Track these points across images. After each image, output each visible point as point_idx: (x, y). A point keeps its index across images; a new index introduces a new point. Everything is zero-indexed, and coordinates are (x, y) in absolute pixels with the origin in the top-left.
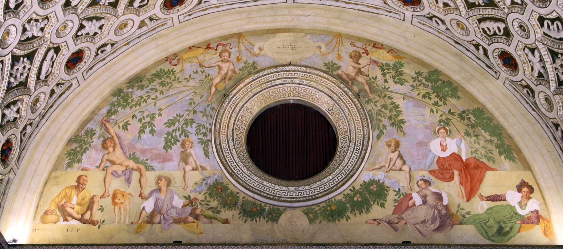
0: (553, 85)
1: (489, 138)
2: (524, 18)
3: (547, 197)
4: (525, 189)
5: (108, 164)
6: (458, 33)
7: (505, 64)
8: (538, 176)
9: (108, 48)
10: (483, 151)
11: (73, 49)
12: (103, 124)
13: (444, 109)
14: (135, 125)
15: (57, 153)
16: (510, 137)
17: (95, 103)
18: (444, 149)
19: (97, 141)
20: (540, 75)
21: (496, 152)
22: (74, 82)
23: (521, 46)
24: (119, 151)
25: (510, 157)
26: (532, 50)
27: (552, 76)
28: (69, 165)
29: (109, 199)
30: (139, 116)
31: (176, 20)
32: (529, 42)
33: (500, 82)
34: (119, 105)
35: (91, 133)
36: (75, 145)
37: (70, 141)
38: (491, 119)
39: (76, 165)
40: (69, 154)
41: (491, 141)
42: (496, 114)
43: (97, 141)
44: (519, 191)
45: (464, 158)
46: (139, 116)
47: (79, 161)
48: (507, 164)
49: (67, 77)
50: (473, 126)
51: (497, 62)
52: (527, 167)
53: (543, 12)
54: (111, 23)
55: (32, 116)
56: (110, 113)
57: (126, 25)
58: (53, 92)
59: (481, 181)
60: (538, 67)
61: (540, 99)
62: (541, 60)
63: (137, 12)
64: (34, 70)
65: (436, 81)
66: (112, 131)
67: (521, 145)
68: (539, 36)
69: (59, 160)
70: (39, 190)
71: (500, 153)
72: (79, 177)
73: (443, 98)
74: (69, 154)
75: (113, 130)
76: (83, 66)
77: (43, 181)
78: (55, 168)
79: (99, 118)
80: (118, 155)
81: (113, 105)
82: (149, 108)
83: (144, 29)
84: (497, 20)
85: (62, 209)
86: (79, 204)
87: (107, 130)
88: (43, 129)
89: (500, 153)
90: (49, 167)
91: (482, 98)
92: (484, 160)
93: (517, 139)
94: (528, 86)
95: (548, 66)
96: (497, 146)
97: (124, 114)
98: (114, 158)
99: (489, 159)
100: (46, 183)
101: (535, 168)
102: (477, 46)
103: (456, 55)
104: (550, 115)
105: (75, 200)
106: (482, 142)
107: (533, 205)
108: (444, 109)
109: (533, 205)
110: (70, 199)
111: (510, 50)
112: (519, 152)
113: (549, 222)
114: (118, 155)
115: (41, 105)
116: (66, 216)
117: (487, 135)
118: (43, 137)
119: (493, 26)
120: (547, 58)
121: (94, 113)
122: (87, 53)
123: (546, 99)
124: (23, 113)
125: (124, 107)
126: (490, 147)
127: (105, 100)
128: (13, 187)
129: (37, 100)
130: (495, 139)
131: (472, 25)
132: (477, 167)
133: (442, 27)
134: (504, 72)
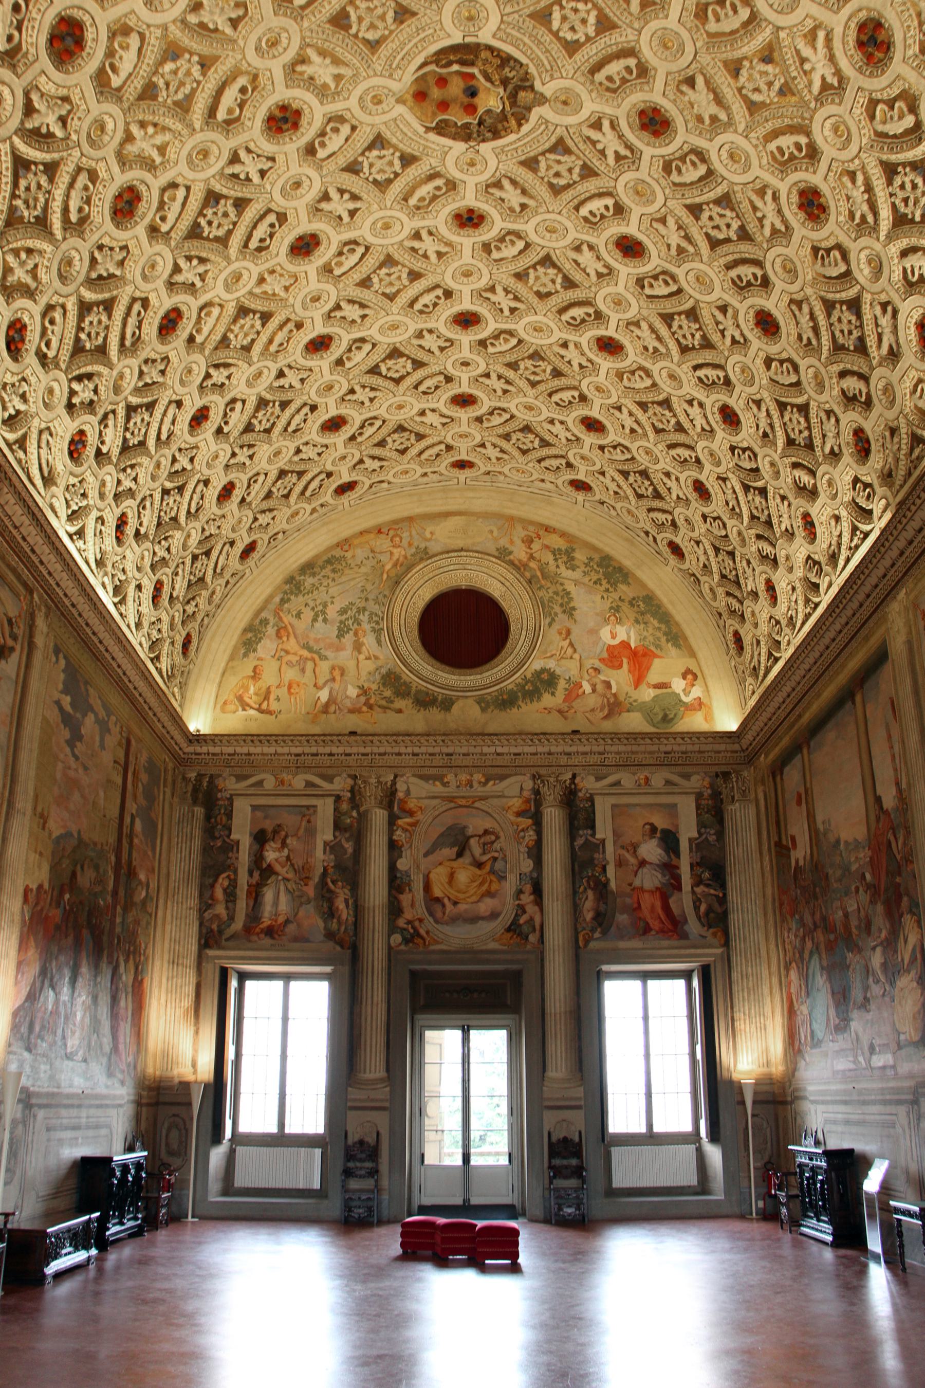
0: (716, 577)
1: (657, 625)
2: (689, 513)
3: (710, 684)
4: (690, 677)
5: (283, 653)
6: (629, 520)
7: (673, 553)
8: (702, 663)
9: (280, 536)
10: (651, 638)
11: (247, 540)
12: (276, 613)
13: (615, 596)
14: (308, 615)
15: (233, 643)
16: (677, 624)
17: (269, 591)
18: (614, 637)
19: (271, 630)
20: (705, 566)
21: (664, 639)
22: (248, 571)
23: (687, 538)
24: (292, 640)
25: (677, 645)
26: (698, 543)
27: (715, 569)
28: (245, 655)
29: (285, 689)
30: (312, 604)
31: (346, 504)
32: (695, 535)
33: (669, 569)
34: (292, 593)
35: (265, 622)
36: (250, 635)
37: (245, 631)
38: (659, 606)
39: (252, 655)
40: (245, 644)
41: (659, 629)
42: (665, 601)
43: (271, 630)
44: (684, 678)
45: (633, 646)
46: (312, 604)
47: (255, 650)
48: (673, 651)
49: (241, 568)
50: (643, 614)
51: (666, 551)
52: (693, 654)
53: (706, 510)
54: (283, 513)
55: (209, 608)
56: (283, 601)
57: (297, 513)
58: (228, 582)
59: (648, 668)
60: (702, 559)
61: (706, 589)
62: (705, 553)
63: (309, 501)
64: (212, 565)
65: (607, 567)
66: (285, 619)
67: (688, 633)
68: (703, 531)
69: (235, 650)
70: (218, 680)
71: (668, 641)
72: (255, 668)
73: (614, 584)
74: (245, 644)
75: (287, 619)
76: (255, 555)
77: (221, 671)
78: (232, 658)
79: (272, 607)
80: (292, 645)
81: (285, 593)
82: (321, 596)
83: (315, 515)
84: (664, 511)
85: (240, 699)
86: (256, 694)
87: (280, 619)
88: (218, 619)
89: (668, 641)
90: (226, 657)
91: (652, 584)
92: (652, 648)
93: (684, 626)
94: (694, 575)
95: (712, 559)
96: (665, 634)
97: (297, 602)
98: (288, 648)
99: (657, 646)
100: (224, 673)
101: (700, 655)
102: (647, 533)
103: (627, 540)
104: (714, 604)
105: (252, 690)
106: (650, 630)
107: (697, 692)
108: (615, 596)
109: (697, 692)
110: (247, 689)
111: (678, 540)
112: (686, 639)
113: (710, 708)
114: (292, 645)
115: (217, 598)
116: (245, 706)
117: (656, 623)
118: (219, 627)
119: (662, 517)
120: (711, 553)
121: (268, 601)
122: (260, 543)
123: (711, 589)
124: (201, 607)
125: (296, 595)
126: (659, 634)
127: (278, 588)
128: (193, 677)
129: (213, 593)
130: (663, 626)
131: (642, 514)
132: (644, 655)
133: (613, 513)
134: (673, 560)
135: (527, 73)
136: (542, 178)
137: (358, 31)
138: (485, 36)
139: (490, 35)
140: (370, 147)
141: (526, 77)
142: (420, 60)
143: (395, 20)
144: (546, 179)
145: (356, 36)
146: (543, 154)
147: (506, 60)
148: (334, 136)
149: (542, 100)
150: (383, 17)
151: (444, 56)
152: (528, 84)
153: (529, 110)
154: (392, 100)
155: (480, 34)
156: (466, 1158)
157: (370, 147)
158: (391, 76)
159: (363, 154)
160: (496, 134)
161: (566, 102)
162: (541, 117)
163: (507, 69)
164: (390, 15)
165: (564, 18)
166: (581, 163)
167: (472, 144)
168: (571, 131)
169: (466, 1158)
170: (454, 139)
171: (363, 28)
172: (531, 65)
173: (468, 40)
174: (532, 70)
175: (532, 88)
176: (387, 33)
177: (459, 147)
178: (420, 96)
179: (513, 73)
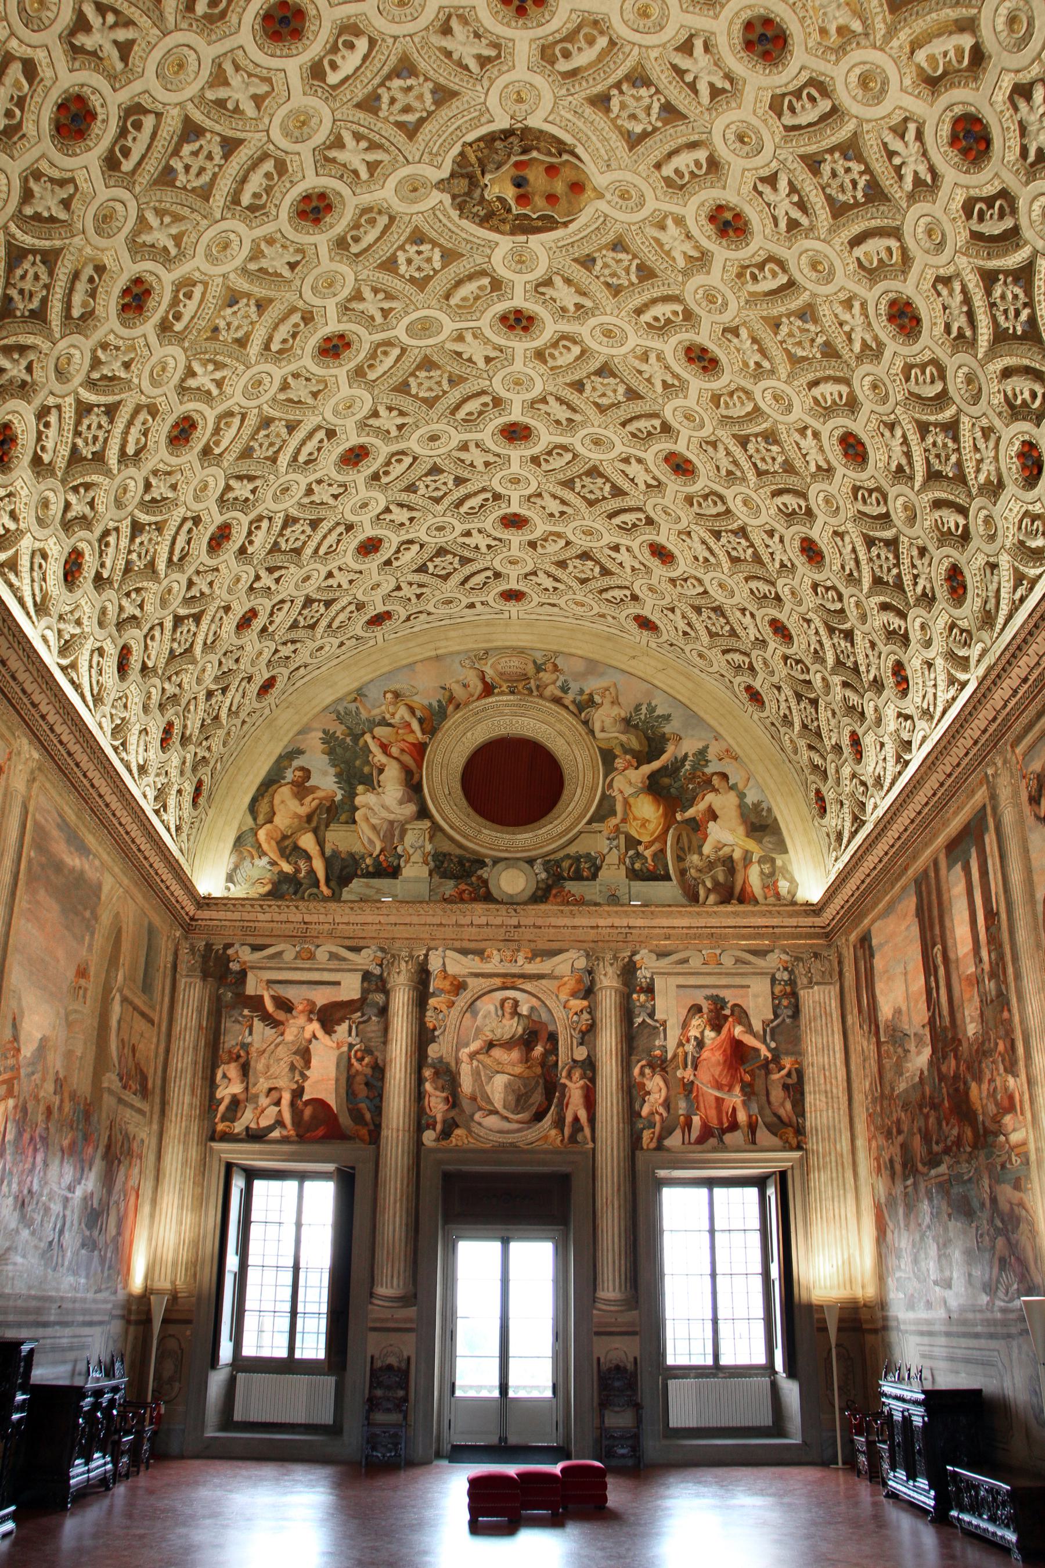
135: (461, 210)
136: (427, 79)
137: (631, 261)
138: (506, 243)
139: (501, 245)
140: (645, 135)
141: (461, 208)
142: (573, 227)
143: (594, 260)
144: (421, 79)
145: (635, 256)
146: (430, 114)
147: (484, 221)
148: (683, 168)
149: (441, 185)
150: (606, 266)
151: (549, 224)
152: (459, 200)
153: (452, 175)
154: (608, 196)
155: (511, 245)
156: (504, 1387)
157: (645, 135)
158: (606, 216)
159: (655, 129)
160: (490, 139)
161: (414, 188)
162: (439, 167)
163: (482, 213)
164: (598, 267)
165: (429, 260)
166: (381, 114)
167: (519, 125)
168: (401, 158)
169: (504, 1387)
170: (541, 132)
171: (627, 263)
172: (456, 218)
173: (523, 238)
174: (455, 214)
175: (454, 197)
176: (604, 252)
177: (535, 122)
178: (577, 187)
179: (475, 210)
